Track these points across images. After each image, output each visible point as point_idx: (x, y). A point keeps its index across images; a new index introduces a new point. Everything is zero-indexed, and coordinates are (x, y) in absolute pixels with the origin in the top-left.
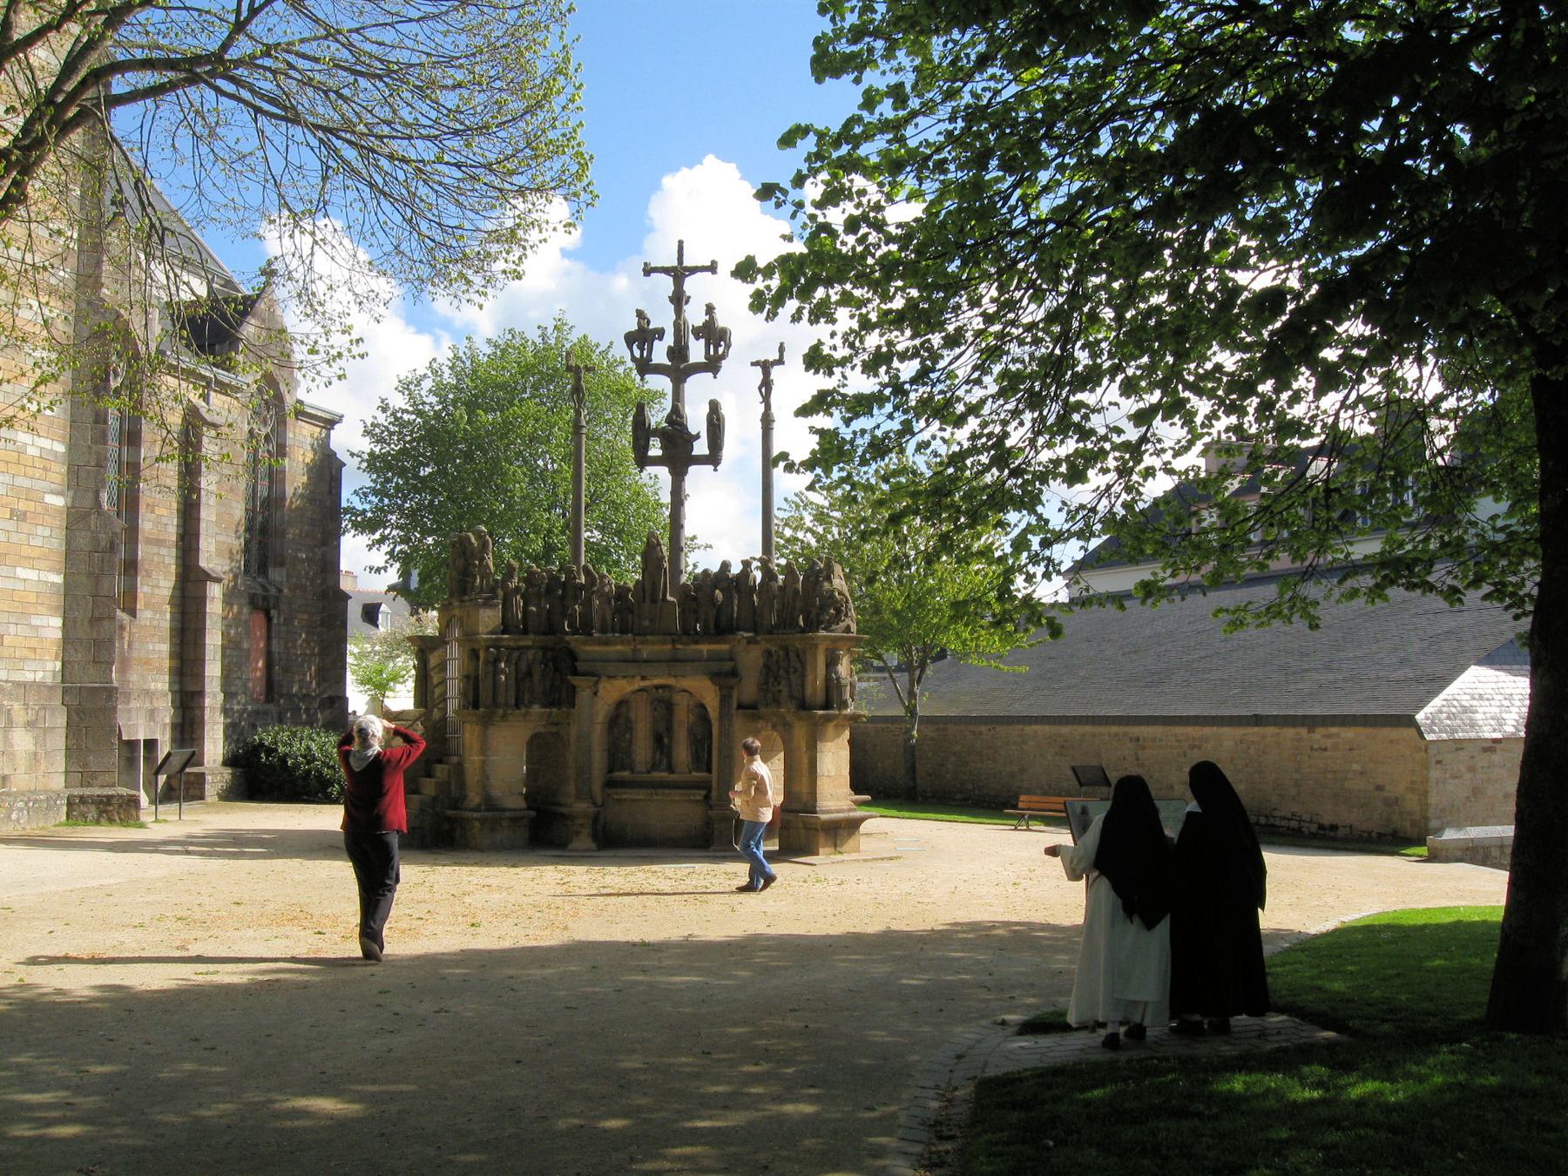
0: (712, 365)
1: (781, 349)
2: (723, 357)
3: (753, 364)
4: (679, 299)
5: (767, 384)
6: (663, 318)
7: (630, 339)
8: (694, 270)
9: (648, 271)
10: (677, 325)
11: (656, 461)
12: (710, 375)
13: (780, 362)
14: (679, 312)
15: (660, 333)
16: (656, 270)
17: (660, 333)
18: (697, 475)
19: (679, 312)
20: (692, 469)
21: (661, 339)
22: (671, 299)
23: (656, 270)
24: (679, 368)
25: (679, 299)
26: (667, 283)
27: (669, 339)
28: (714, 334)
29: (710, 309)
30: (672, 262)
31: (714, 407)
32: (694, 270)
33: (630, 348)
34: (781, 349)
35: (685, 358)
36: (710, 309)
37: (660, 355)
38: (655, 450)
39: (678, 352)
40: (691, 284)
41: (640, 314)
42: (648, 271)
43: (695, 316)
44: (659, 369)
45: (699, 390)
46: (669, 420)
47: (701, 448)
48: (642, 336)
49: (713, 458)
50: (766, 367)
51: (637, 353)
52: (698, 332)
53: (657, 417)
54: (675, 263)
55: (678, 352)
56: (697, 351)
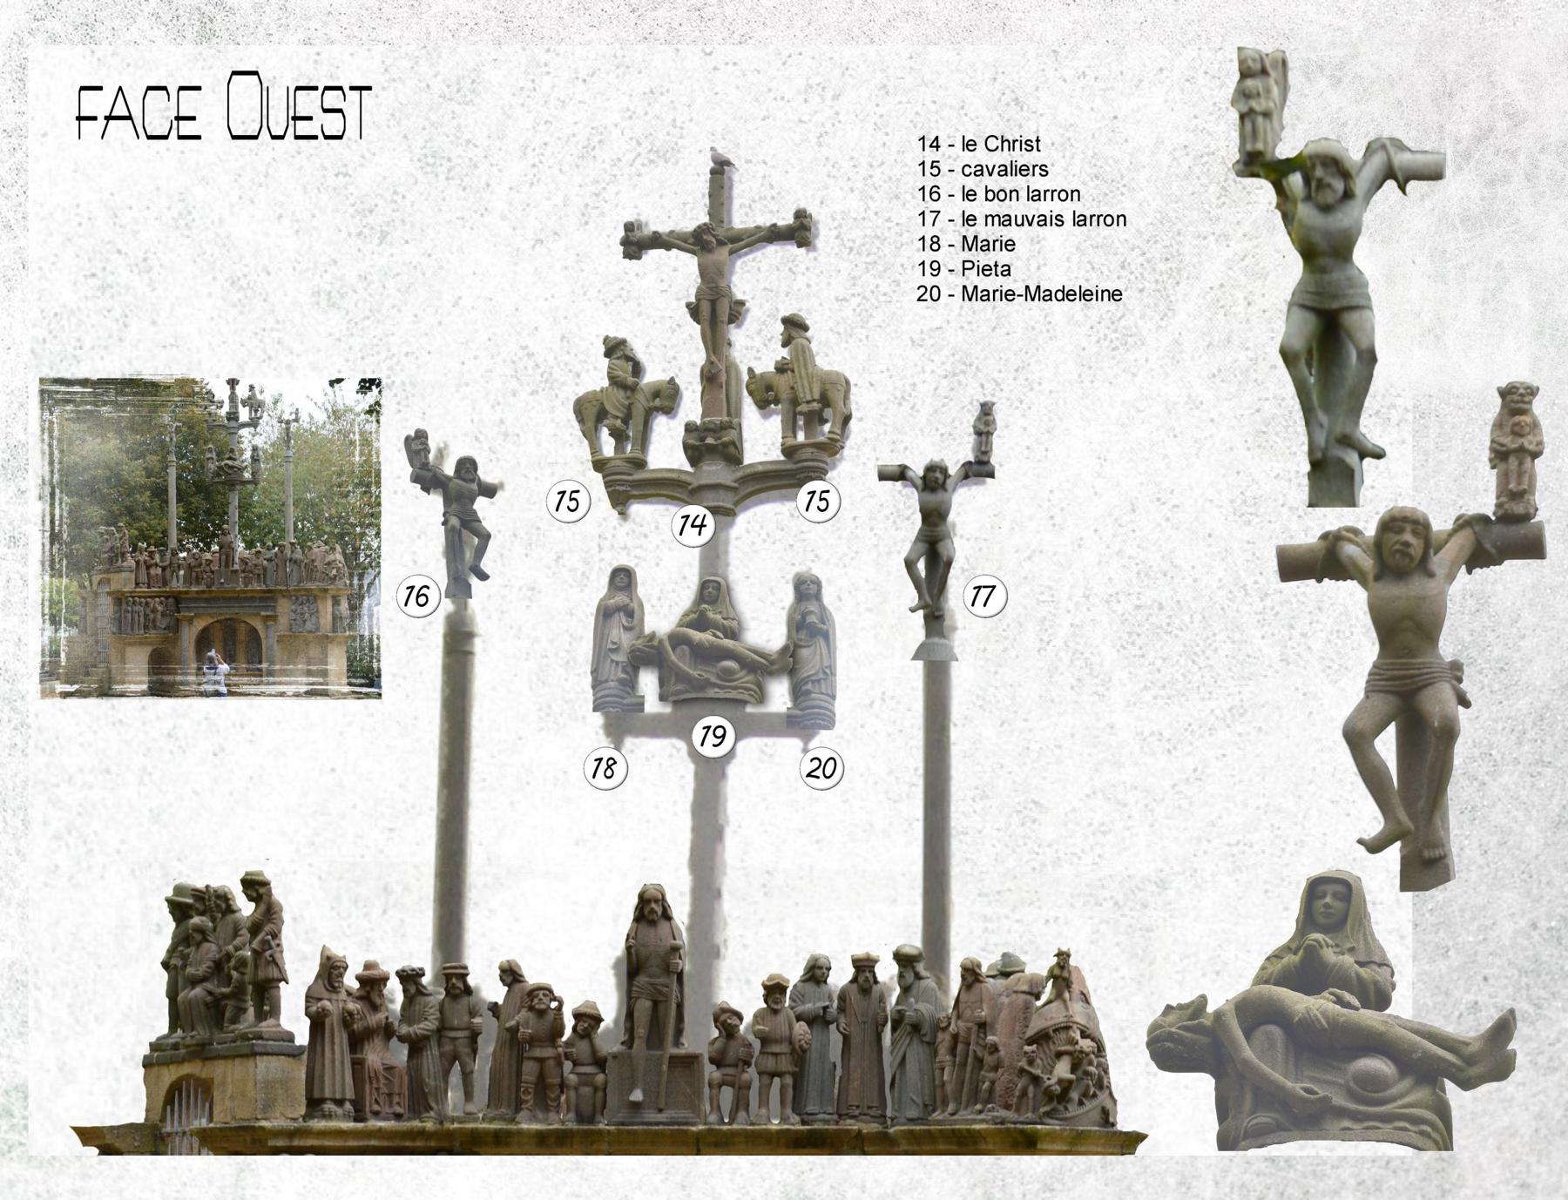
0: (798, 470)
1: (984, 427)
6: (672, 354)
7: (590, 413)
10: (710, 378)
19: (715, 342)
22: (694, 311)
25: (715, 311)
27: (691, 408)
30: (694, 216)
33: (591, 436)
37: (666, 449)
41: (615, 348)
43: (755, 348)
44: (668, 488)
48: (620, 406)
51: (608, 446)
55: (712, 442)
56: (762, 438)
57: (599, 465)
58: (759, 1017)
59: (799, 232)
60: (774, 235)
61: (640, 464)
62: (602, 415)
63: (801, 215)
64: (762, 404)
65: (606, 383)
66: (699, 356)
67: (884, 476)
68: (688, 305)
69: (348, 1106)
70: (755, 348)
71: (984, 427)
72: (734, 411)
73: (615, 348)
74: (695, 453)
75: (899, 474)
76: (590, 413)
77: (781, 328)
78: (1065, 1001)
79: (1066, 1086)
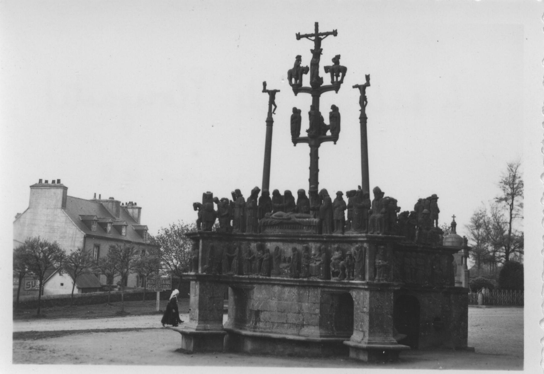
0: (336, 87)
3: (354, 87)
4: (317, 53)
5: (363, 101)
9: (299, 37)
11: (303, 140)
18: (325, 148)
24: (317, 89)
25: (317, 53)
31: (335, 109)
34: (368, 78)
39: (317, 81)
42: (299, 37)
43: (326, 60)
44: (306, 90)
45: (327, 100)
49: (335, 138)
50: (362, 89)
52: (327, 69)
54: (314, 32)
70: (326, 60)
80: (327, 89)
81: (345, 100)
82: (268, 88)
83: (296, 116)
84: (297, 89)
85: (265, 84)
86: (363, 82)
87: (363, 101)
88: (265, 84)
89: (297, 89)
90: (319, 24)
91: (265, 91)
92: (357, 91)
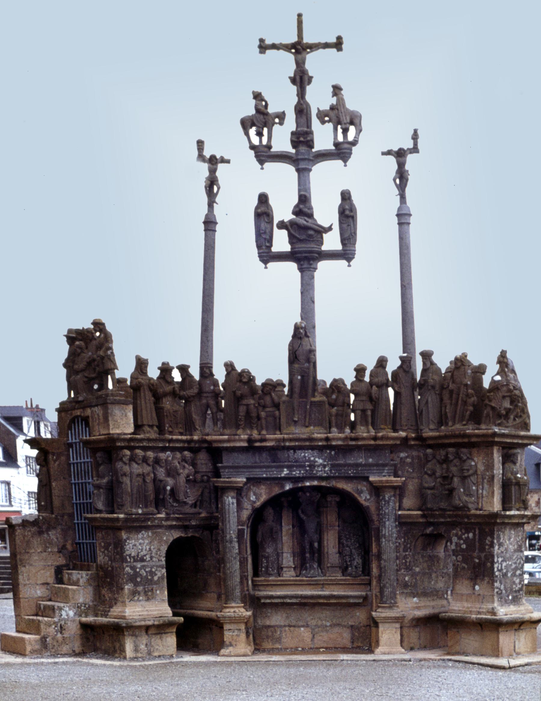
1: (415, 136)
2: (354, 143)
4: (301, 79)
5: (402, 176)
7: (246, 124)
8: (313, 47)
9: (263, 47)
11: (281, 257)
12: (340, 162)
13: (415, 150)
14: (301, 94)
15: (281, 116)
16: (274, 47)
17: (281, 116)
19: (301, 94)
20: (323, 267)
21: (281, 123)
22: (293, 81)
23: (274, 47)
24: (303, 154)
25: (301, 79)
26: (287, 62)
27: (291, 123)
28: (340, 116)
29: (337, 90)
30: (293, 38)
32: (313, 47)
33: (247, 134)
35: (310, 144)
36: (337, 90)
37: (281, 139)
38: (281, 242)
39: (302, 138)
40: (313, 62)
41: (257, 96)
43: (319, 98)
46: (298, 212)
47: (332, 242)
51: (255, 140)
52: (321, 116)
53: (283, 210)
55: (302, 138)
56: (323, 137)
57: (253, 147)
58: (352, 384)
59: (338, 45)
60: (326, 46)
61: (269, 147)
62: (253, 125)
63: (339, 38)
64: (323, 122)
65: (254, 112)
66: (295, 100)
67: (383, 154)
68: (290, 78)
69: (155, 428)
71: (415, 136)
72: (309, 125)
73: (257, 96)
74: (295, 144)
75: (389, 153)
76: (246, 124)
77: (332, 89)
78: (505, 373)
79: (508, 411)
80: (324, 156)
81: (365, 176)
82: (207, 154)
83: (263, 211)
84: (264, 155)
85: (200, 144)
86: (408, 144)
87: (402, 176)
88: (200, 144)
89: (264, 155)
90: (304, 18)
91: (201, 157)
92: (392, 162)
